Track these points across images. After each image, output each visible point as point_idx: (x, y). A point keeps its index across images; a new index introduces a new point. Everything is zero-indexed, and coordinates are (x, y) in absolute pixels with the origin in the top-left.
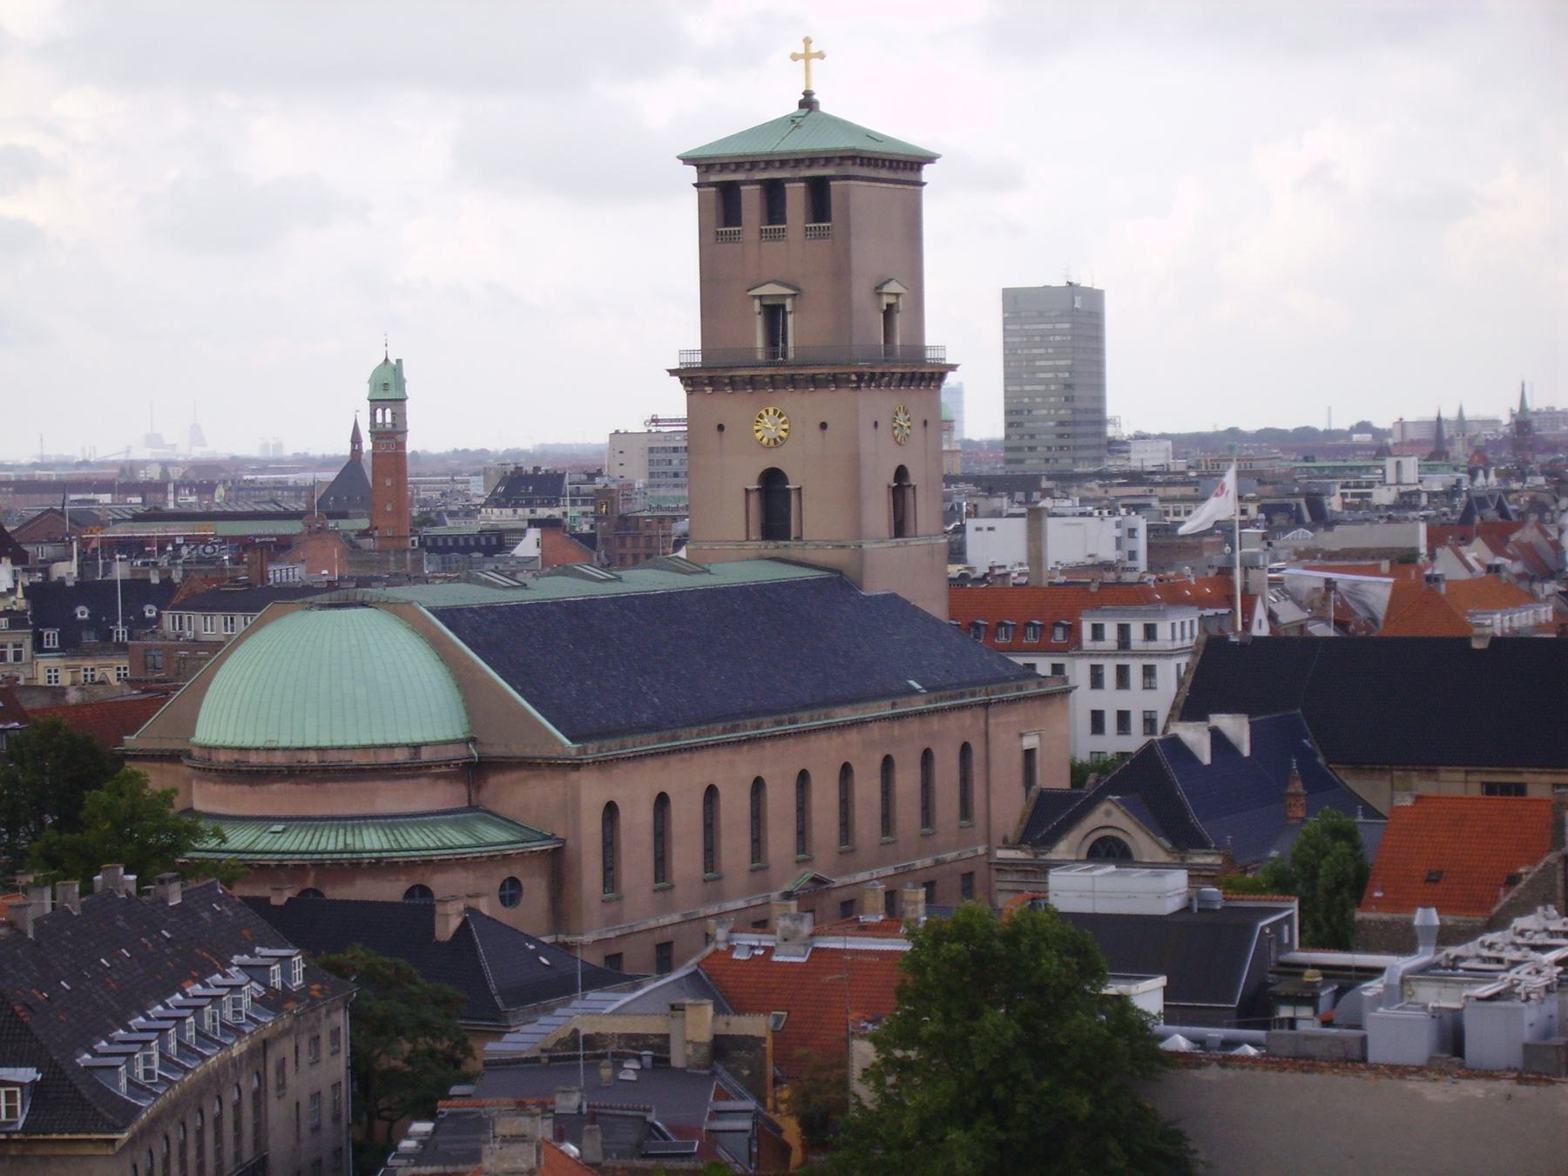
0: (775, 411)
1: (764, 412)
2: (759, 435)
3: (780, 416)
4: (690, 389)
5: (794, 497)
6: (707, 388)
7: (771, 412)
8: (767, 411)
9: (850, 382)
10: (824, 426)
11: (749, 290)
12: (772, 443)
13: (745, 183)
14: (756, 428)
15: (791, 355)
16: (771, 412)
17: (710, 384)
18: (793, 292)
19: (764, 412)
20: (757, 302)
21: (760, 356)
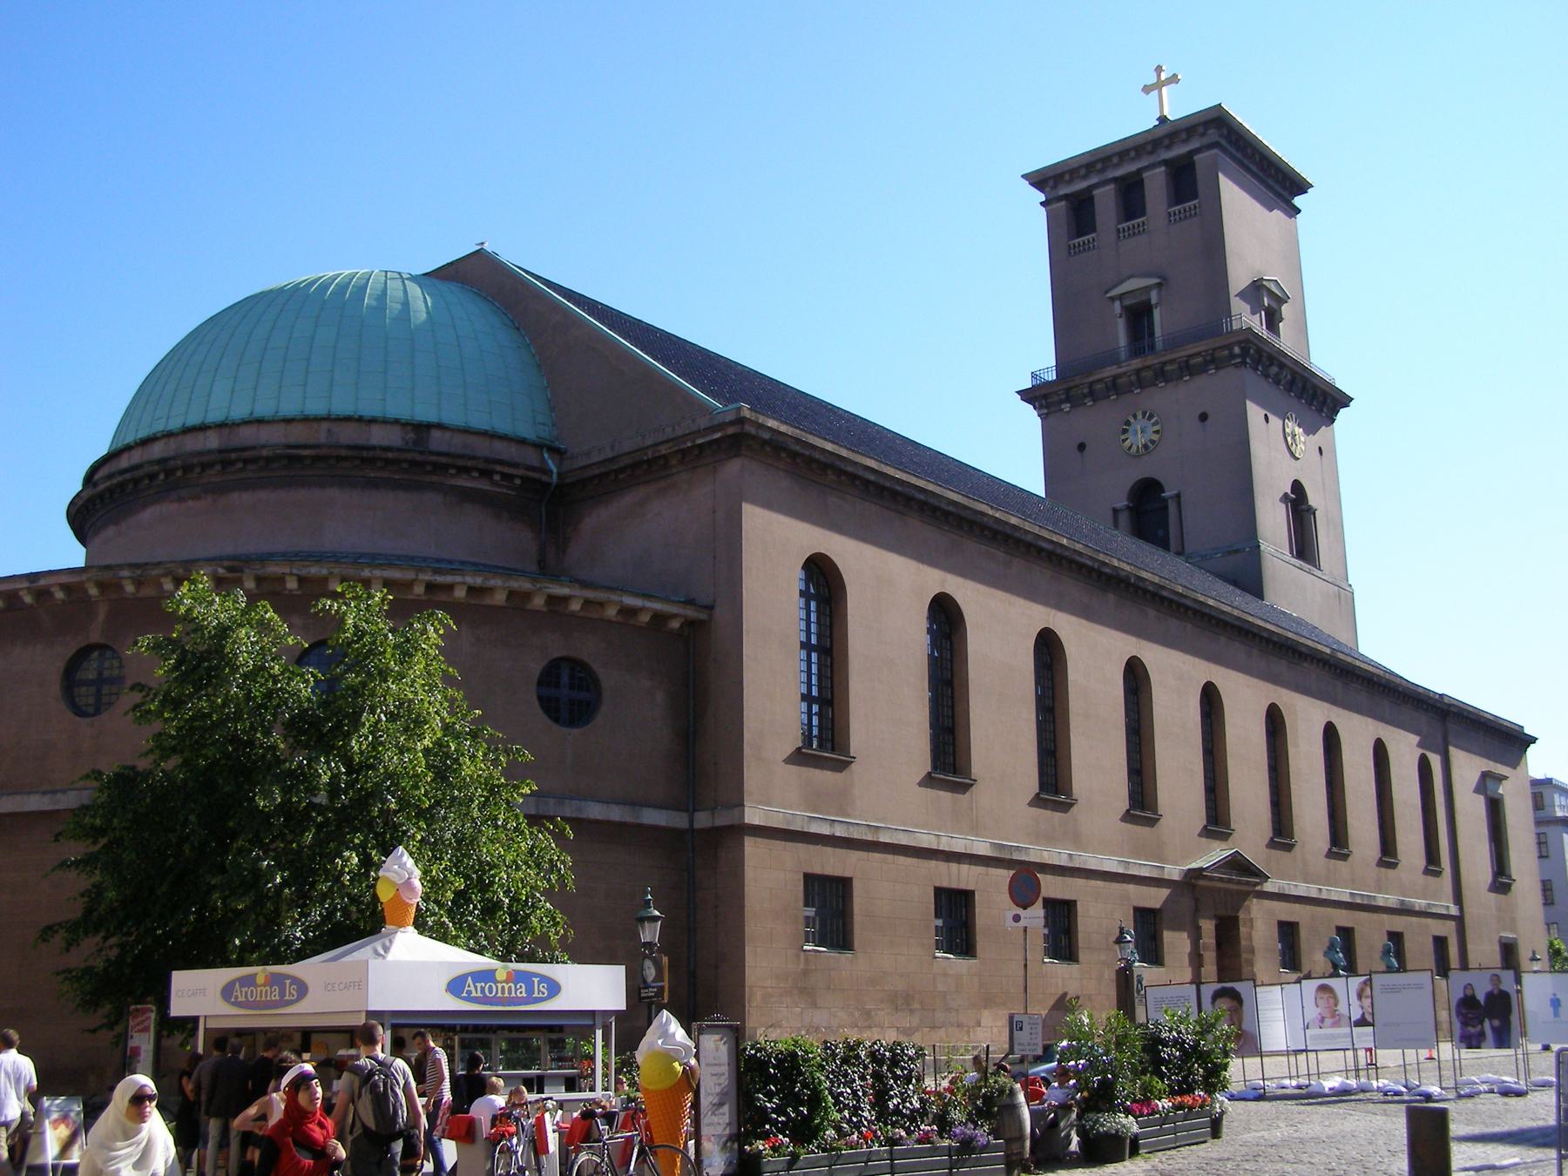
0: (1144, 414)
8: (1135, 416)
9: (1232, 356)
10: (1203, 417)
11: (1106, 292)
14: (1123, 437)
15: (1159, 345)
17: (1067, 400)
18: (1157, 281)
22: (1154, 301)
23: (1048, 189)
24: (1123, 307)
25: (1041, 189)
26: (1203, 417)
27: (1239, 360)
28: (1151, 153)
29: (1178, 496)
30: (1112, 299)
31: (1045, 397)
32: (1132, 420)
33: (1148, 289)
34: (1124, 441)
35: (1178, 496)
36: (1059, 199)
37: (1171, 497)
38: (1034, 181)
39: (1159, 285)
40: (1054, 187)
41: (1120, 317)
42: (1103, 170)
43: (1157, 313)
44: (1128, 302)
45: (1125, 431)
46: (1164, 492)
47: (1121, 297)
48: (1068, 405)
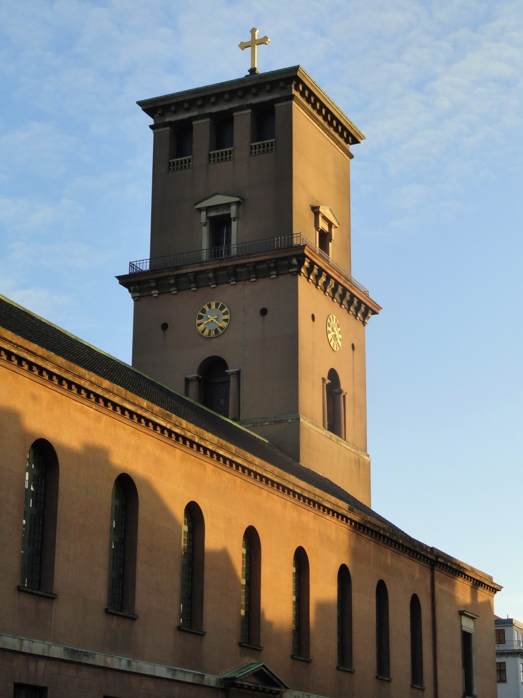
0: (217, 305)
1: (206, 307)
2: (201, 328)
3: (222, 308)
4: (138, 295)
5: (233, 381)
6: (153, 292)
7: (213, 306)
8: (210, 306)
10: (264, 312)
11: (196, 204)
12: (213, 333)
13: (195, 118)
14: (198, 322)
15: (234, 251)
16: (213, 306)
18: (237, 199)
19: (206, 307)
20: (204, 214)
21: (205, 256)
22: (233, 215)
23: (156, 116)
24: (208, 218)
25: (152, 116)
26: (264, 312)
27: (295, 269)
28: (242, 97)
29: (238, 373)
30: (200, 210)
31: (139, 283)
32: (207, 309)
33: (228, 205)
34: (199, 325)
35: (238, 373)
36: (165, 124)
37: (233, 374)
38: (145, 107)
39: (238, 203)
40: (162, 115)
41: (205, 225)
42: (201, 107)
43: (234, 224)
44: (212, 214)
45: (200, 317)
46: (228, 369)
47: (208, 209)
48: (157, 292)
